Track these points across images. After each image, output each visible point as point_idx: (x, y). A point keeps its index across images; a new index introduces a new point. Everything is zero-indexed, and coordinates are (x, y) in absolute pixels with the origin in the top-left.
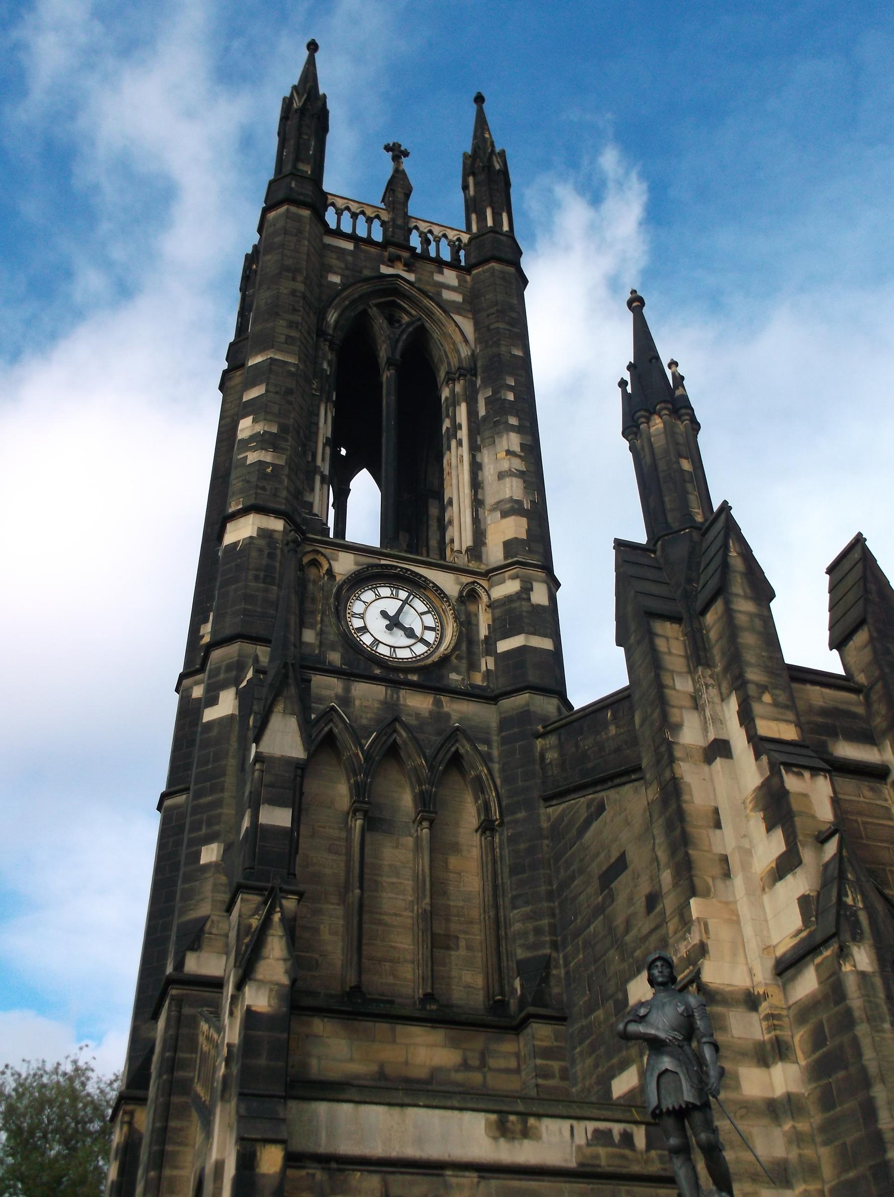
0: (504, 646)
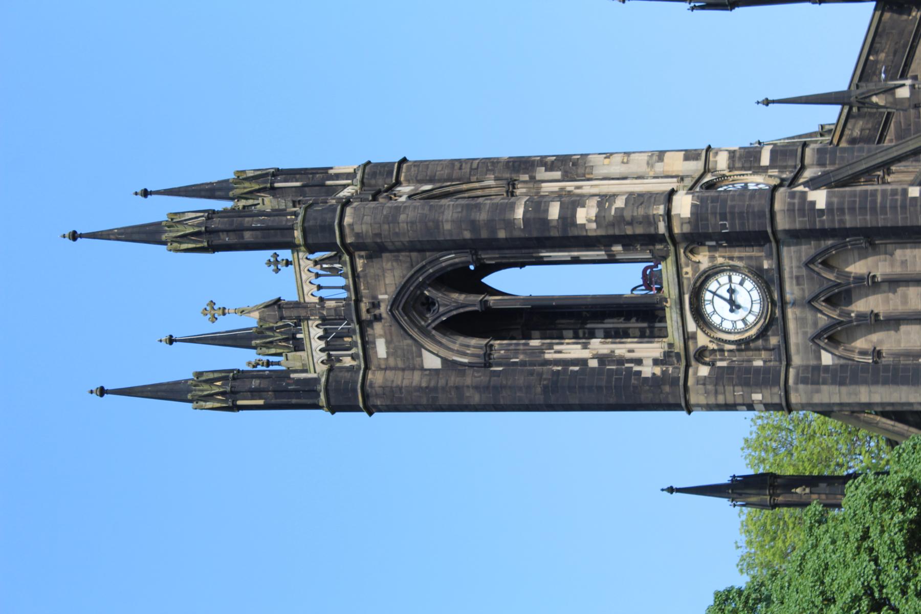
0: (765, 160)
